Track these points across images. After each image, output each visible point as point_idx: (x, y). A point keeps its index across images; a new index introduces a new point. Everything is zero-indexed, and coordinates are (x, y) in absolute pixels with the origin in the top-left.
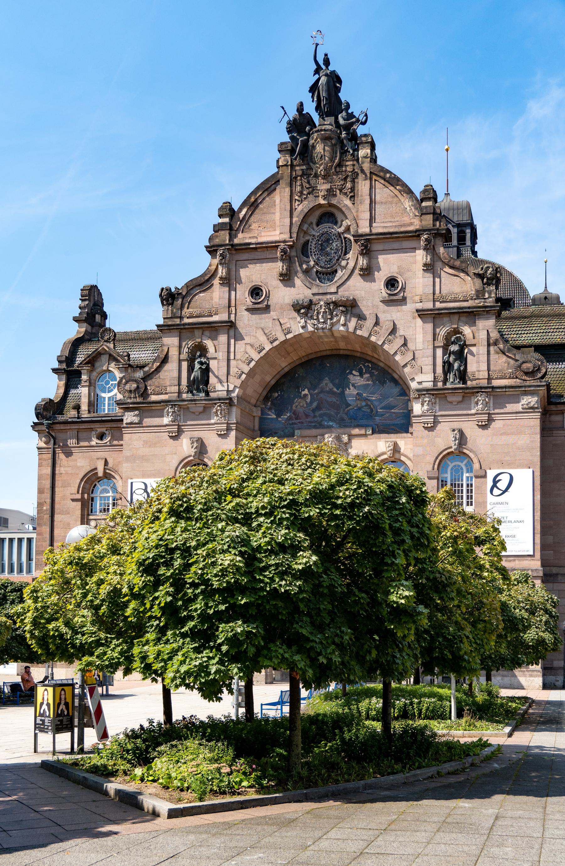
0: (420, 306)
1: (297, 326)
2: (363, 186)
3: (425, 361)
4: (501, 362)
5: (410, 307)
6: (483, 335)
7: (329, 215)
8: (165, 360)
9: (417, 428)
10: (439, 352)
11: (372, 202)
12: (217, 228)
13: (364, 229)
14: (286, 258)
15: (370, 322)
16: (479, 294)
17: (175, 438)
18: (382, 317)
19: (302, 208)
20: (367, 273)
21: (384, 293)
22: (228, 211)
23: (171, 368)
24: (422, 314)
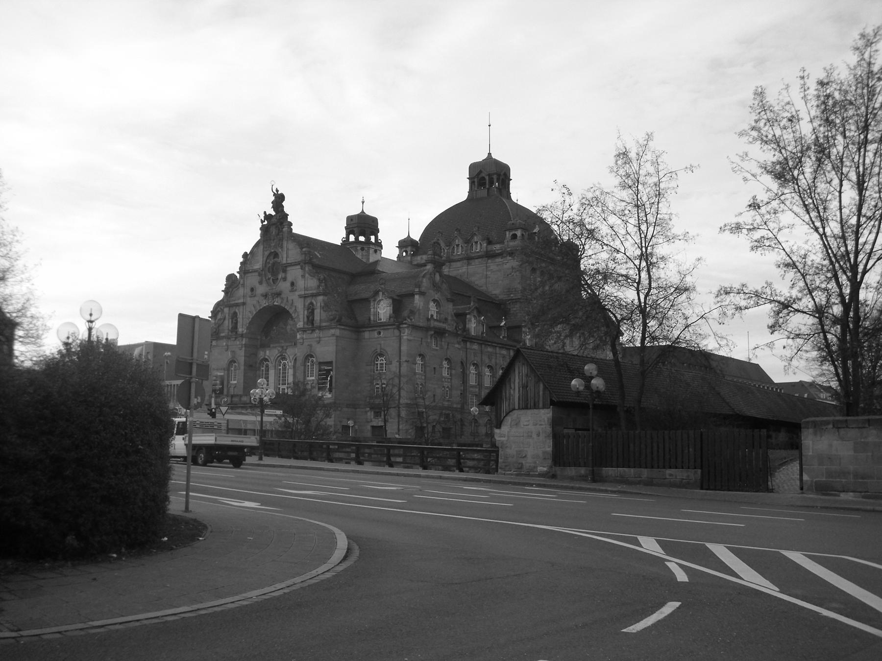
0: (300, 293)
1: (264, 303)
2: (285, 243)
3: (301, 316)
4: (324, 315)
5: (297, 293)
6: (319, 305)
7: (276, 255)
8: (224, 319)
9: (298, 345)
10: (306, 312)
11: (288, 249)
12: (241, 263)
13: (284, 262)
14: (260, 275)
15: (285, 301)
16: (319, 286)
17: (227, 350)
18: (290, 298)
19: (267, 253)
20: (285, 279)
21: (290, 288)
22: (245, 255)
23: (226, 322)
24: (300, 296)
